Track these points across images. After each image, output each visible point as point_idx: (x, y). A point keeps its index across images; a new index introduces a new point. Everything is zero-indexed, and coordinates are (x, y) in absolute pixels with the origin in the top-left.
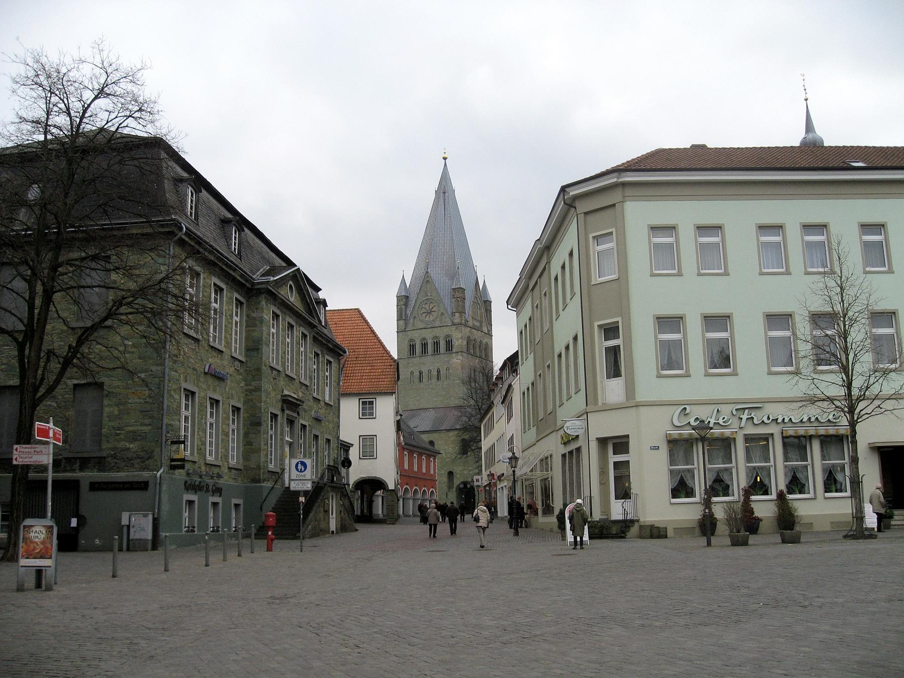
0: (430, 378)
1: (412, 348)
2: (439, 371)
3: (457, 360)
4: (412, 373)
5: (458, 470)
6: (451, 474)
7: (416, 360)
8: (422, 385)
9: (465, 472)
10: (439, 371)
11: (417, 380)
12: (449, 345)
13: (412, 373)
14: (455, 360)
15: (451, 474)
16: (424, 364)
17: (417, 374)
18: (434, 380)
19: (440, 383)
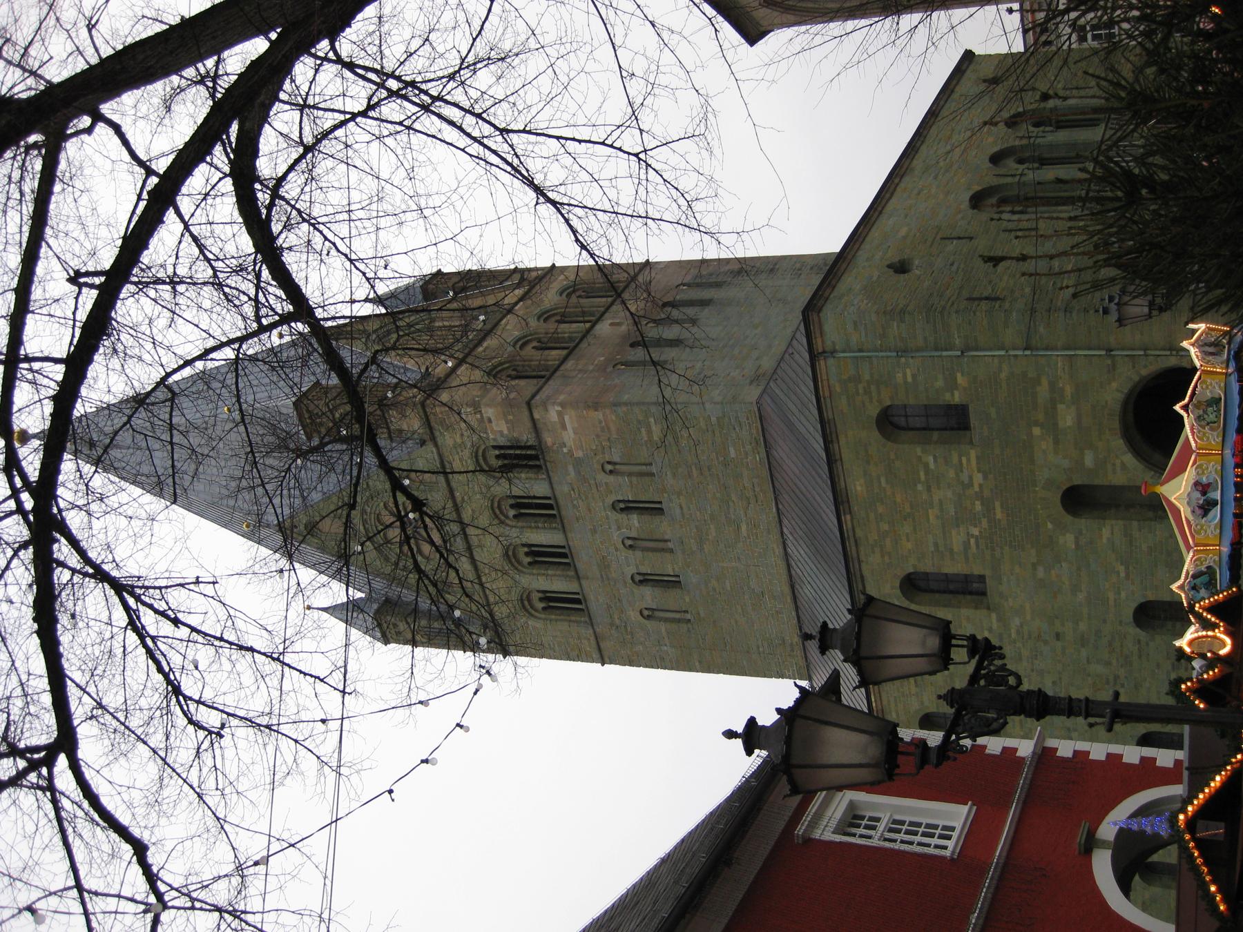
0: (660, 546)
1: (554, 603)
2: (627, 507)
3: (567, 426)
4: (649, 614)
5: (1054, 464)
6: (1079, 499)
7: (597, 597)
8: (691, 578)
9: (1067, 418)
10: (627, 507)
11: (671, 599)
12: (523, 457)
13: (649, 614)
14: (569, 436)
15: (1079, 499)
16: (604, 565)
17: (648, 596)
18: (663, 527)
19: (672, 506)
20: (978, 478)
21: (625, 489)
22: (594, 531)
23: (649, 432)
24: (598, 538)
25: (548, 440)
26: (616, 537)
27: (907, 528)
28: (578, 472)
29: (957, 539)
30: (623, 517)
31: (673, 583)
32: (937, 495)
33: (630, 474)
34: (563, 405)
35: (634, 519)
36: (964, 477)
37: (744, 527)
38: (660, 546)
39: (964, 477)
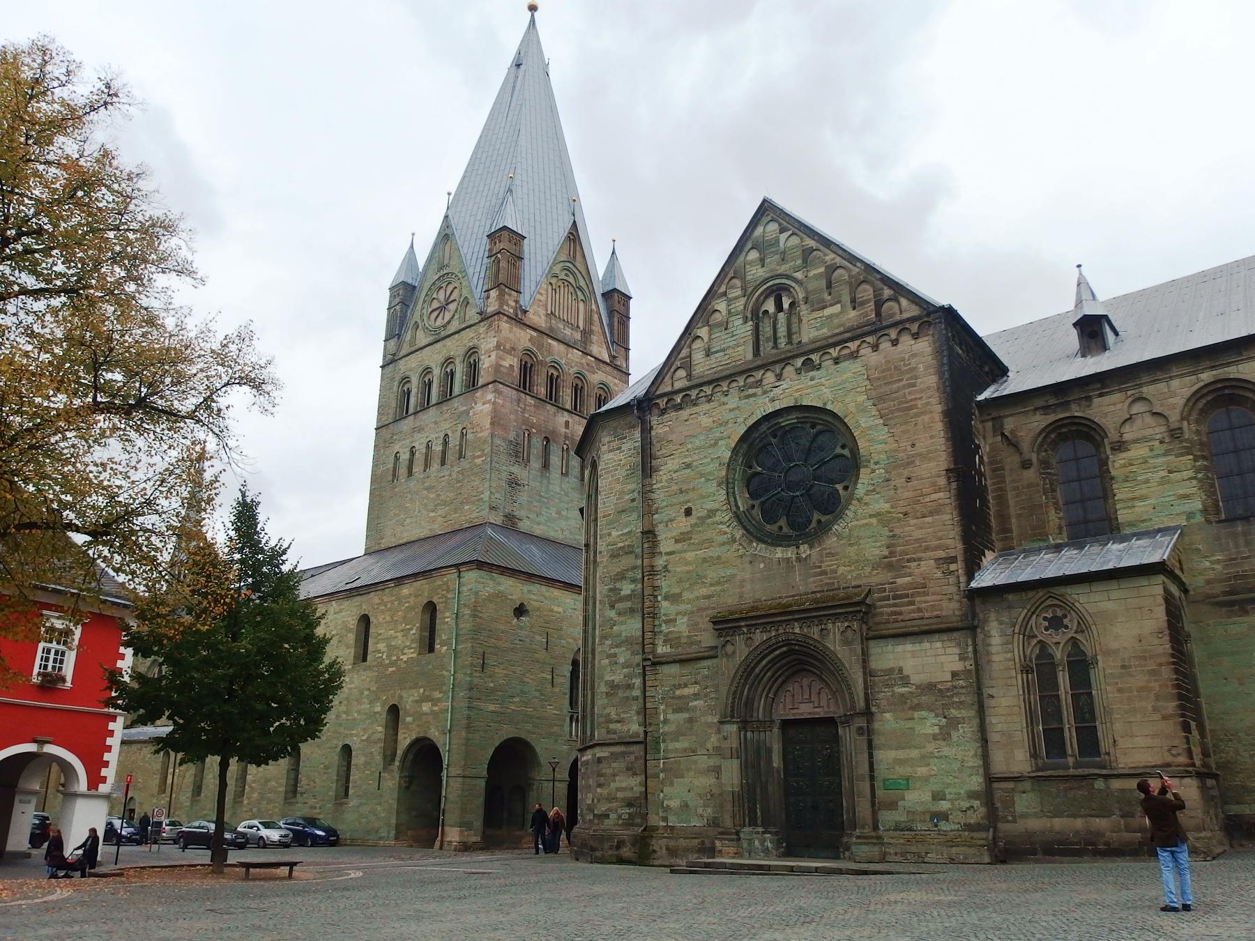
0: (427, 465)
8: (412, 484)
11: (403, 471)
14: (479, 407)
15: (394, 711)
16: (420, 429)
18: (435, 466)
19: (446, 471)
20: (405, 658)
21: (454, 442)
22: (436, 423)
23: (479, 457)
24: (432, 428)
25: (478, 394)
26: (433, 436)
27: (388, 618)
28: (462, 413)
29: (382, 646)
30: (441, 441)
31: (410, 473)
32: (400, 635)
33: (461, 445)
34: (494, 403)
35: (440, 448)
36: (406, 651)
37: (432, 514)
38: (427, 465)
39: (406, 651)
